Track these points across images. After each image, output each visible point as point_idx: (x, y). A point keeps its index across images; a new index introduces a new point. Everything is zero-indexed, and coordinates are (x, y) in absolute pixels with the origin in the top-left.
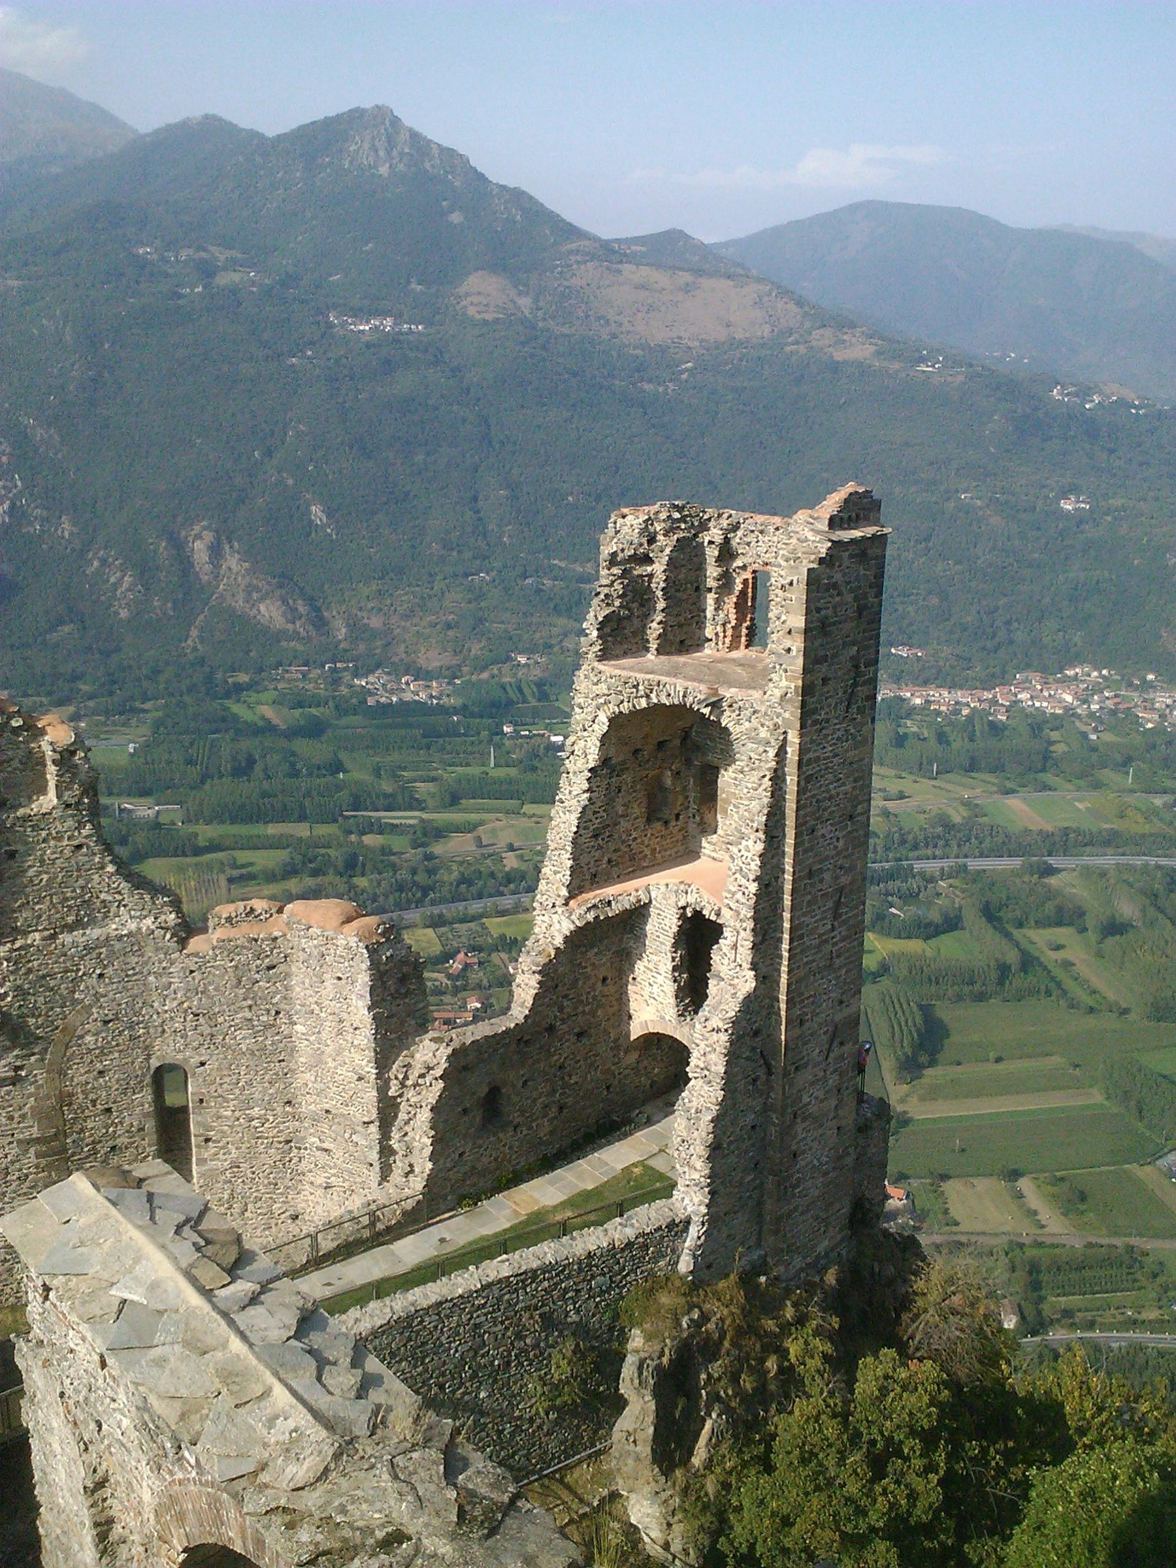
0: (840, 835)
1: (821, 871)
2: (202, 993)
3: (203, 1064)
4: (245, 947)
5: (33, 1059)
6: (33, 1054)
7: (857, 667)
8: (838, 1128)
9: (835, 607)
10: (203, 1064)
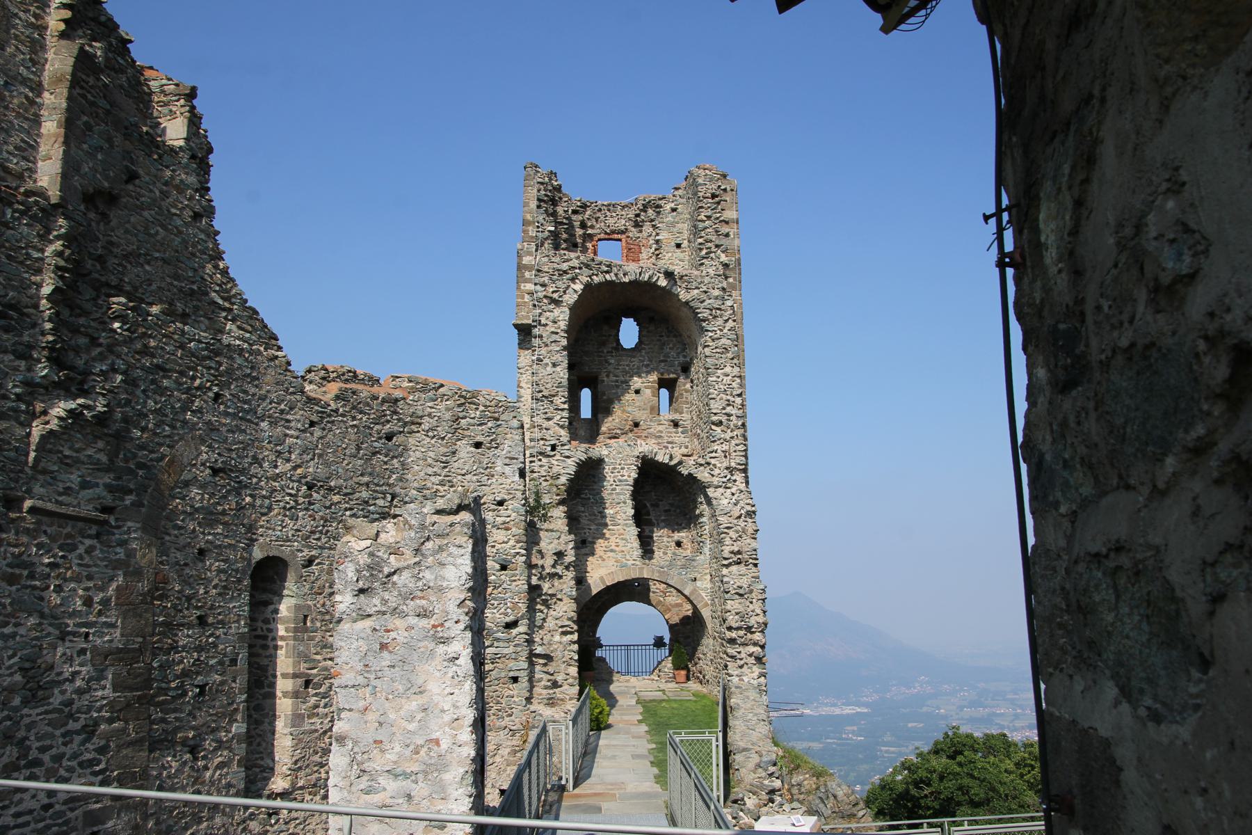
2: (320, 456)
3: (310, 562)
4: (368, 404)
5: (129, 499)
6: (130, 492)
10: (310, 562)
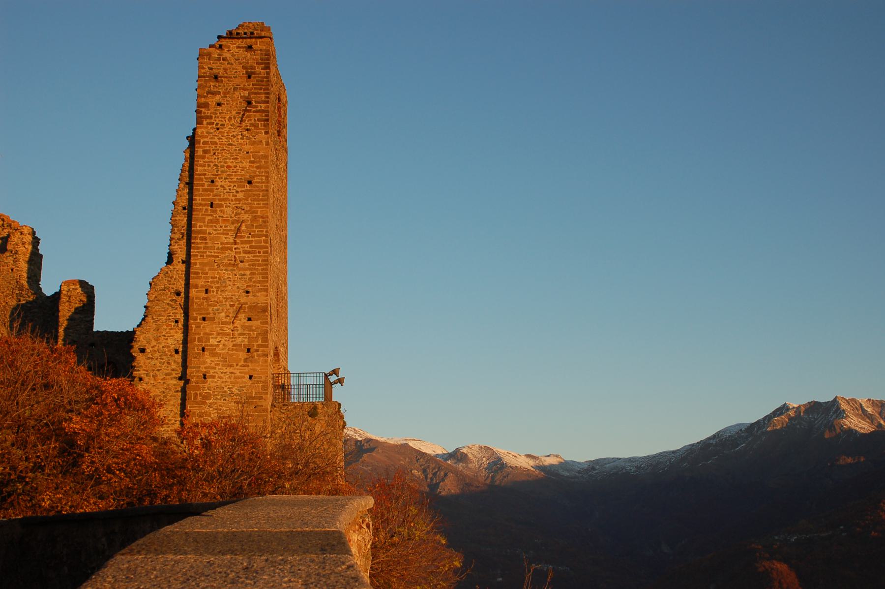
0: (239, 190)
1: (221, 206)
7: (249, 103)
8: (251, 377)
9: (225, 70)
